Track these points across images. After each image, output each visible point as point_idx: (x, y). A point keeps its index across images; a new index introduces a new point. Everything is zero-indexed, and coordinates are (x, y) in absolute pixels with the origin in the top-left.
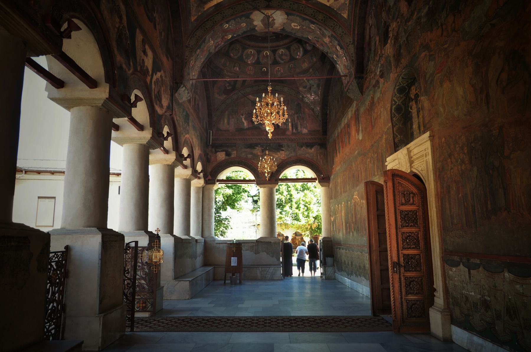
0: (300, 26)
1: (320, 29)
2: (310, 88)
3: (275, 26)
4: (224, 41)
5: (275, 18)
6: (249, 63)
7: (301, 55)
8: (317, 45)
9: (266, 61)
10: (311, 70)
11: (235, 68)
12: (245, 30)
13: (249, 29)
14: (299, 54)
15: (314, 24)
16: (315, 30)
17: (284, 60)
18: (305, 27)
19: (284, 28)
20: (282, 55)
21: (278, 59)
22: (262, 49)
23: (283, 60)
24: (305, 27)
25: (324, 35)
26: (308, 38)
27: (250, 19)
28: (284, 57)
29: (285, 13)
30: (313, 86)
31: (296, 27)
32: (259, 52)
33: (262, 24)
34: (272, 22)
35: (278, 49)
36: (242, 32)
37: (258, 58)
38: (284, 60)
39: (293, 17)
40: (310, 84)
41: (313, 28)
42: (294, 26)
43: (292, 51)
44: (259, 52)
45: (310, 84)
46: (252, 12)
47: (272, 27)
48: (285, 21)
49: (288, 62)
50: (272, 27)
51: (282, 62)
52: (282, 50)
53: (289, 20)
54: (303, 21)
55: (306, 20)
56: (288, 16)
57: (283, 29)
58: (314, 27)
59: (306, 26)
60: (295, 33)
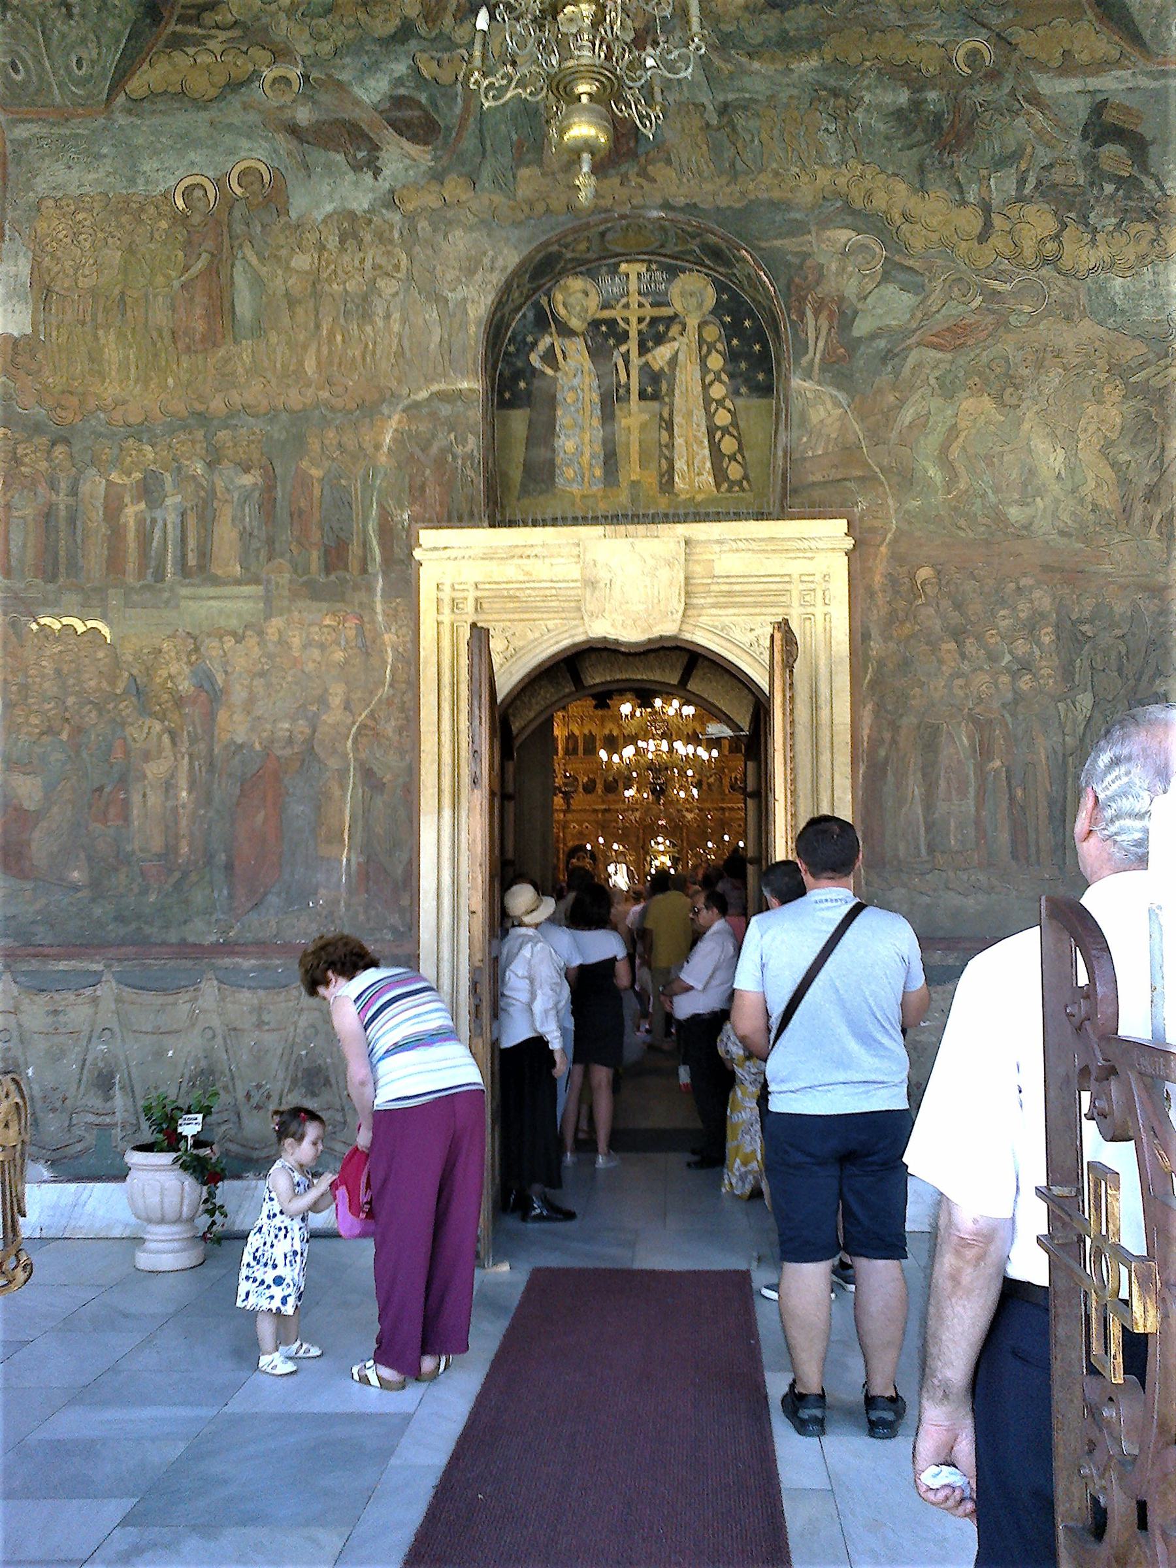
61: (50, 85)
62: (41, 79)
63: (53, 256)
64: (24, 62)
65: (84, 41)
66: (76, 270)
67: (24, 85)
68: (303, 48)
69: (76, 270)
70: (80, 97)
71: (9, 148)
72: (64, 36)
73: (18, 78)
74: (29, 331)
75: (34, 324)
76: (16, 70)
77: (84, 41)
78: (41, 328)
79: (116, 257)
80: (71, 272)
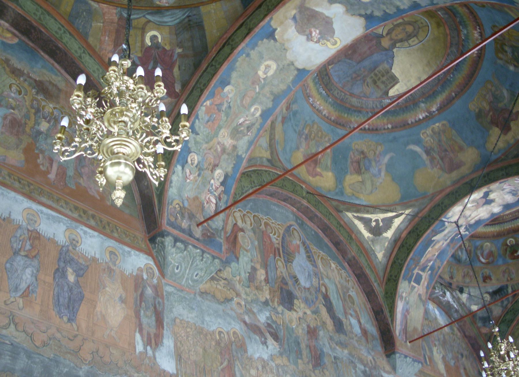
0: (264, 79)
1: (249, 128)
3: (293, 28)
5: (311, 44)
8: (208, 103)
15: (261, 115)
16: (247, 113)
18: (257, 90)
19: (275, 40)
24: (257, 90)
25: (236, 133)
26: (229, 84)
27: (360, 15)
29: (308, 69)
31: (263, 67)
33: (322, 13)
34: (307, 32)
39: (291, 78)
41: (252, 110)
42: (268, 67)
46: (366, 30)
47: (294, 18)
48: (290, 56)
50: (294, 18)
53: (288, 65)
54: (272, 93)
55: (273, 101)
56: (298, 70)
57: (271, 35)
58: (253, 115)
59: (259, 93)
60: (248, 55)
61: (184, 277)
62: (183, 274)
63: (181, 342)
64: (181, 267)
65: (201, 269)
66: (189, 351)
67: (176, 274)
68: (244, 296)
69: (189, 351)
70: (190, 285)
71: (165, 294)
72: (197, 265)
73: (176, 271)
74: (175, 372)
75: (177, 370)
76: (177, 269)
77: (201, 269)
78: (179, 372)
79: (201, 351)
80: (187, 352)
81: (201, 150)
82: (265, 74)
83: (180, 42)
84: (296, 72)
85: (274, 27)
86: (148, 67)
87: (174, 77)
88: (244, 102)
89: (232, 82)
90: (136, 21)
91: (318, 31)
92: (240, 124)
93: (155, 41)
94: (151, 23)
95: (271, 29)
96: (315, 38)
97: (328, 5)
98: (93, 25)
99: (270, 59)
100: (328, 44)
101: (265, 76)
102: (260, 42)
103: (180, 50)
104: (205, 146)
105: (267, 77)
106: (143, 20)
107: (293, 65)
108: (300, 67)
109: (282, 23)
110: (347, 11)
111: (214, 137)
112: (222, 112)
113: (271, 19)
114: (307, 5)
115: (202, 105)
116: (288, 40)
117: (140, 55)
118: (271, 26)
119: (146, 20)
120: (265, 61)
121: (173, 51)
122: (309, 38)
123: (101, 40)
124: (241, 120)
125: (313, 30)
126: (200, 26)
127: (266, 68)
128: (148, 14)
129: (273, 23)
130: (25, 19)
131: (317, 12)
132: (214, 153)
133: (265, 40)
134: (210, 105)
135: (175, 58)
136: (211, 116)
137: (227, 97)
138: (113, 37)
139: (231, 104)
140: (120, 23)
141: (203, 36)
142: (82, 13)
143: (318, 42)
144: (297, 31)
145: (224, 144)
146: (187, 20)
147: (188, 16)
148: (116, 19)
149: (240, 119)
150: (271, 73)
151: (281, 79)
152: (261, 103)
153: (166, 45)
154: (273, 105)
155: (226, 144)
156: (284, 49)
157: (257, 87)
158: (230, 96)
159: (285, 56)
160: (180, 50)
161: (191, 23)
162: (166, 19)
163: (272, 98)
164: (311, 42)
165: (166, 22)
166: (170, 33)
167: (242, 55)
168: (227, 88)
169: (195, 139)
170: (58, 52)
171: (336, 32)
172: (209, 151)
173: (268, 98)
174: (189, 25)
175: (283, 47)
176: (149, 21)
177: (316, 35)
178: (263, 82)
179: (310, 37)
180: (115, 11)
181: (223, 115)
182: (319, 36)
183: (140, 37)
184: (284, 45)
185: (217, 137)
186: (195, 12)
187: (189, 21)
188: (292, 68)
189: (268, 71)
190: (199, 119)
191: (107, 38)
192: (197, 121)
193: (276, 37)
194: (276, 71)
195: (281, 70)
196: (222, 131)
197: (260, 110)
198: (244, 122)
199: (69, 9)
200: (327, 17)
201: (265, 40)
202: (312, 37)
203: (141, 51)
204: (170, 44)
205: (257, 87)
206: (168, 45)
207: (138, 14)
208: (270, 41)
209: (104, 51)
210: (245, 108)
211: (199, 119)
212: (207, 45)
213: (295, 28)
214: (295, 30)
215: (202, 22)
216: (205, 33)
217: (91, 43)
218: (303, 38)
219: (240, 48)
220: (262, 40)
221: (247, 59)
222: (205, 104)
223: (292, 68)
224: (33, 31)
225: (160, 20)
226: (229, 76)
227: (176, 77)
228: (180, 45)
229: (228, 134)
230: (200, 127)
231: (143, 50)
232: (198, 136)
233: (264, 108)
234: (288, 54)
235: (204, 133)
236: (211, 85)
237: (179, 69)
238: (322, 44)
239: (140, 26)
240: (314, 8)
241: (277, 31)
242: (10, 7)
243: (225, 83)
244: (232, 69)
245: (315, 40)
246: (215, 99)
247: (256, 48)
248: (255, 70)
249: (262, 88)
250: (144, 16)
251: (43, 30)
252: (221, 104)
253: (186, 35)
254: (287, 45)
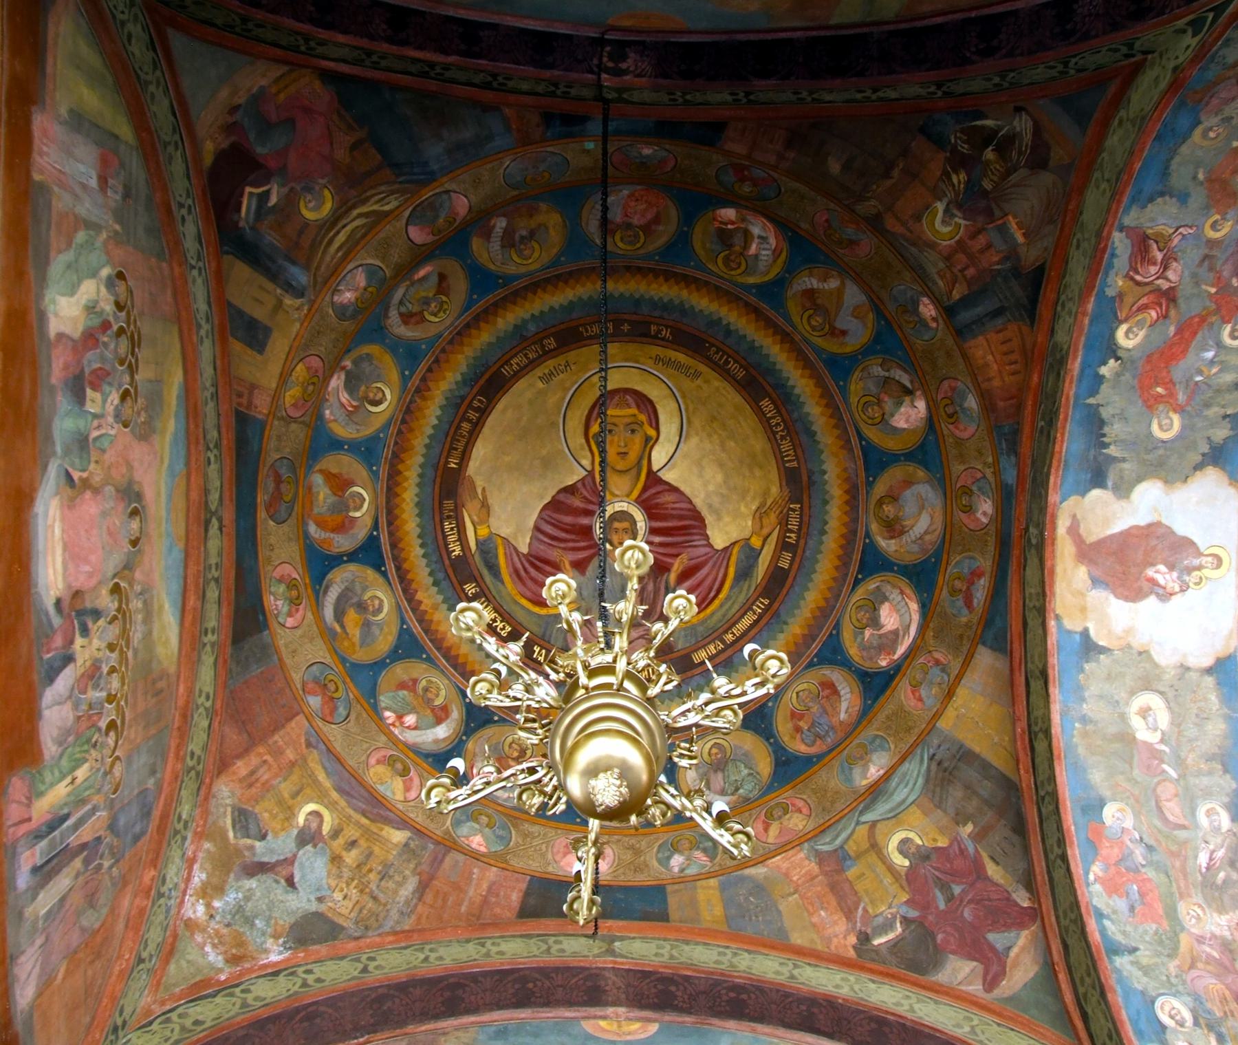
0: (1162, 741)
2: (258, 868)
3: (1112, 598)
4: (1129, 300)
6: (331, 376)
7: (411, 737)
8: (1096, 869)
9: (321, 497)
10: (398, 836)
11: (361, 279)
12: (1115, 430)
13: (1113, 451)
14: (410, 719)
17: (343, 627)
18: (1173, 773)
20: (361, 607)
21: (339, 579)
22: (383, 472)
23: (339, 615)
24: (1173, 773)
26: (1102, 804)
28: (352, 616)
30: (290, 882)
31: (1136, 722)
32: (366, 450)
35: (384, 574)
36: (1105, 413)
37: (337, 445)
38: (343, 627)
39: (1213, 697)
40: (290, 861)
43: (400, 671)
44: (366, 450)
45: (290, 861)
47: (1096, 582)
48: (1165, 658)
49: (343, 660)
51: (329, 613)
52: (380, 594)
54: (1210, 758)
55: (1226, 771)
56: (1209, 671)
57: (1088, 647)
59: (1182, 776)
60: (1084, 720)
81: (1173, 980)
82: (1155, 730)
83: (957, 814)
84: (1209, 681)
85: (1079, 629)
86: (937, 908)
87: (997, 885)
88: (1171, 818)
89: (1107, 793)
90: (851, 842)
91: (1162, 568)
92: (1208, 869)
93: (913, 850)
94: (879, 826)
95: (1077, 637)
96: (1170, 584)
97: (1123, 503)
98: (781, 908)
99: (1133, 693)
100: (1206, 572)
101: (1158, 735)
102: (1081, 677)
103: (969, 828)
104: (1172, 966)
105: (1163, 733)
106: (862, 830)
107: (1188, 669)
108: (1208, 662)
109: (1083, 610)
110: (1167, 482)
111: (1176, 935)
112: (1143, 870)
113: (1057, 617)
114: (1091, 539)
115: (1088, 885)
116: (1129, 631)
117: (905, 897)
118: (1069, 632)
119: (866, 827)
120: (1127, 704)
121: (956, 840)
122: (1165, 595)
123: (814, 925)
124: (1203, 859)
125: (1150, 572)
126: (966, 756)
127: (1144, 718)
128: (862, 813)
129: (1068, 624)
130: (645, 975)
131: (1121, 533)
132: (1210, 968)
133: (1087, 666)
134: (1106, 870)
135: (971, 849)
136: (1128, 894)
137: (1123, 830)
138: (834, 903)
139: (1146, 839)
140: (828, 869)
141: (985, 766)
142: (746, 899)
143: (1184, 588)
144: (1127, 599)
145: (1214, 936)
146: (934, 767)
147: (932, 758)
148: (813, 867)
149: (1196, 857)
150: (1163, 718)
151: (1197, 715)
152: (1208, 794)
153: (935, 840)
154: (1234, 778)
155: (1217, 932)
156: (1140, 653)
157: (1165, 767)
158: (1129, 823)
159: (1156, 665)
160: (969, 828)
161: (946, 765)
162: (897, 798)
163: (1220, 767)
164: (1173, 597)
165: (904, 801)
166: (926, 814)
167: (1074, 728)
168: (1110, 813)
169: (1135, 963)
170: (744, 996)
171: (1195, 539)
172: (1194, 973)
173: (1210, 773)
174: (945, 771)
175: (1134, 652)
176: (874, 824)
177: (1167, 576)
178: (1167, 749)
179: (1161, 591)
180: (802, 855)
181: (1150, 873)
182: (1175, 574)
183: (880, 863)
184: (1129, 646)
185: (1183, 929)
186: (936, 742)
187: (939, 764)
188: (1194, 676)
189: (1155, 720)
190: (1108, 917)
191: (823, 913)
192: (1107, 923)
193: (1101, 643)
194: (1169, 708)
195: (1173, 700)
196: (1182, 908)
197: (1219, 809)
198: (1211, 859)
199: (718, 911)
200: (1150, 526)
201: (1087, 666)
202: (1164, 588)
203: (902, 887)
204: (942, 830)
205: (1165, 767)
206: (939, 838)
207: (844, 828)
208: (1098, 661)
209: (835, 940)
210: (1184, 827)
211: (1108, 917)
212: (1004, 776)
213: (1117, 596)
214: (1121, 602)
215: (961, 746)
216: (983, 760)
217: (799, 942)
218: (1152, 600)
219: (1056, 718)
220: (1082, 670)
221: (1089, 727)
222: (1091, 877)
223: (1194, 676)
224: (673, 988)
225: (888, 806)
226: (1087, 786)
227: (1002, 882)
228: (960, 818)
229: (1200, 906)
230: (1124, 933)
231: (904, 883)
232: (1138, 953)
233: (1226, 800)
234: (1156, 658)
235: (1147, 939)
236: (1069, 830)
237: (998, 864)
238: (1196, 584)
239: (865, 845)
240: (1109, 532)
241: (1092, 633)
242: (604, 969)
243: (1094, 807)
244: (1079, 769)
245: (1177, 589)
246: (1104, 852)
247: (1087, 694)
248: (1127, 738)
249: (1179, 763)
250: (858, 823)
251: (689, 973)
252: (1125, 857)
253: (956, 793)
254: (1137, 642)
